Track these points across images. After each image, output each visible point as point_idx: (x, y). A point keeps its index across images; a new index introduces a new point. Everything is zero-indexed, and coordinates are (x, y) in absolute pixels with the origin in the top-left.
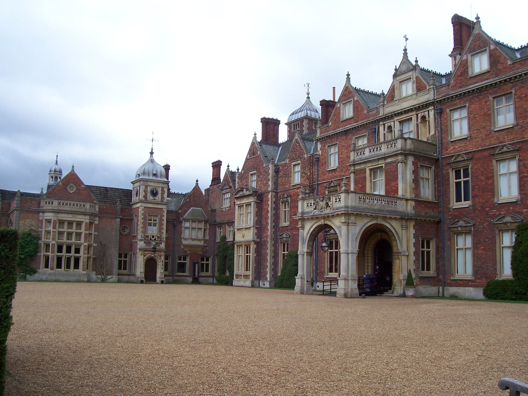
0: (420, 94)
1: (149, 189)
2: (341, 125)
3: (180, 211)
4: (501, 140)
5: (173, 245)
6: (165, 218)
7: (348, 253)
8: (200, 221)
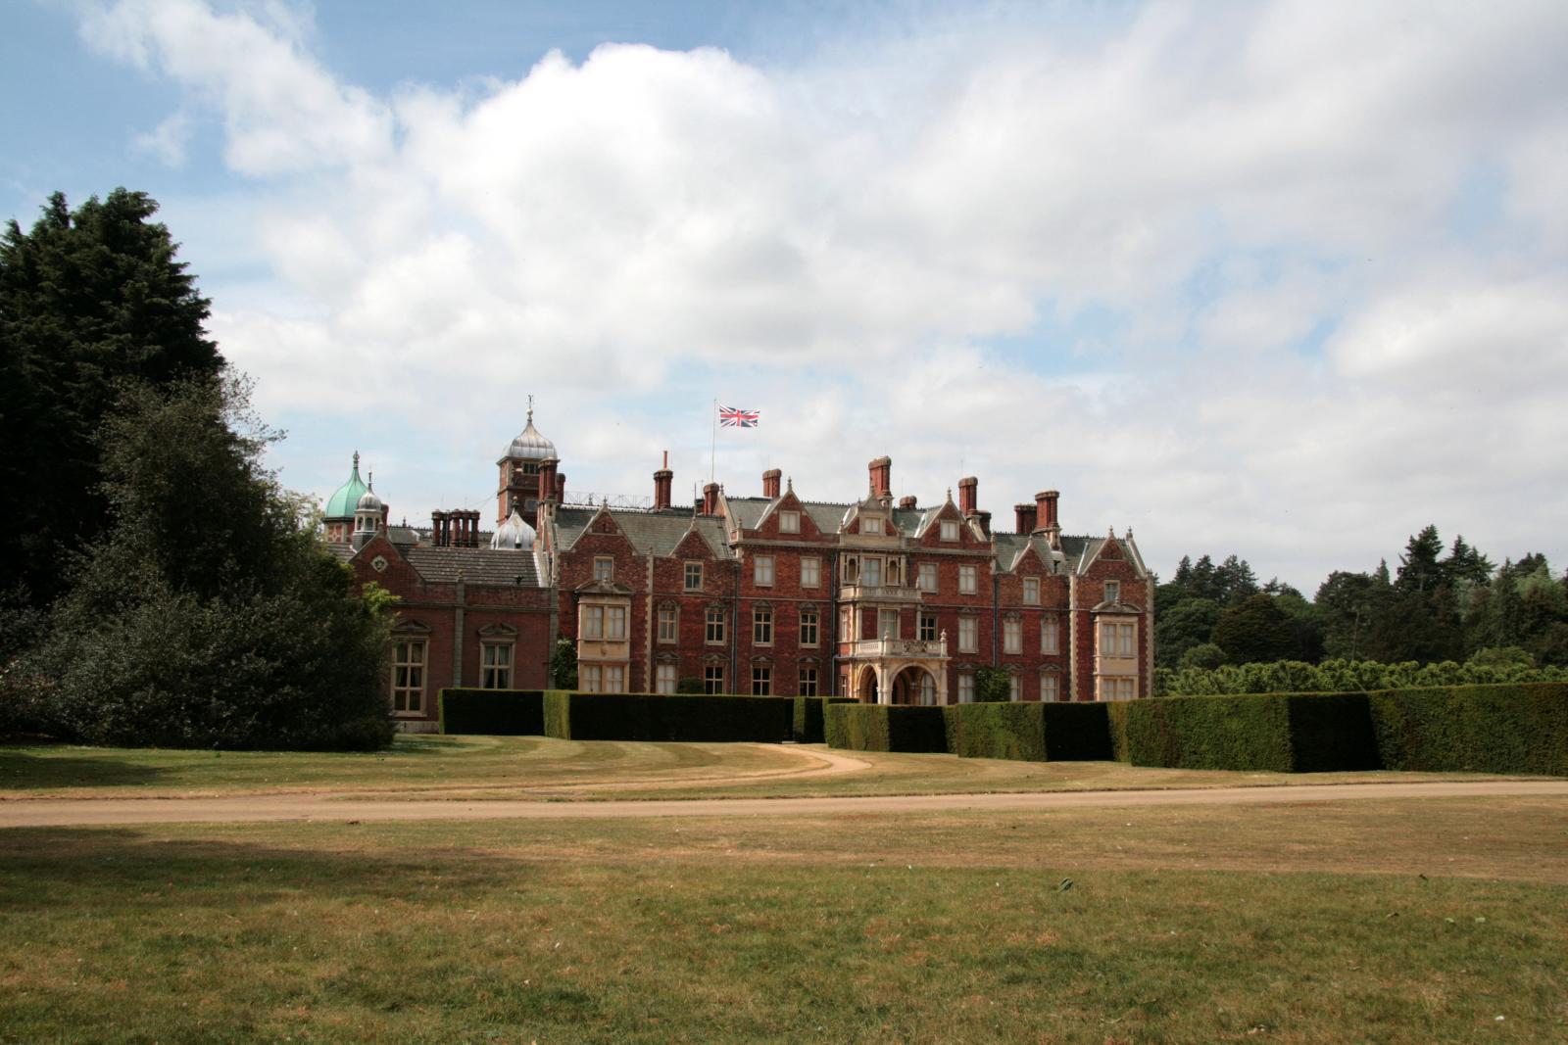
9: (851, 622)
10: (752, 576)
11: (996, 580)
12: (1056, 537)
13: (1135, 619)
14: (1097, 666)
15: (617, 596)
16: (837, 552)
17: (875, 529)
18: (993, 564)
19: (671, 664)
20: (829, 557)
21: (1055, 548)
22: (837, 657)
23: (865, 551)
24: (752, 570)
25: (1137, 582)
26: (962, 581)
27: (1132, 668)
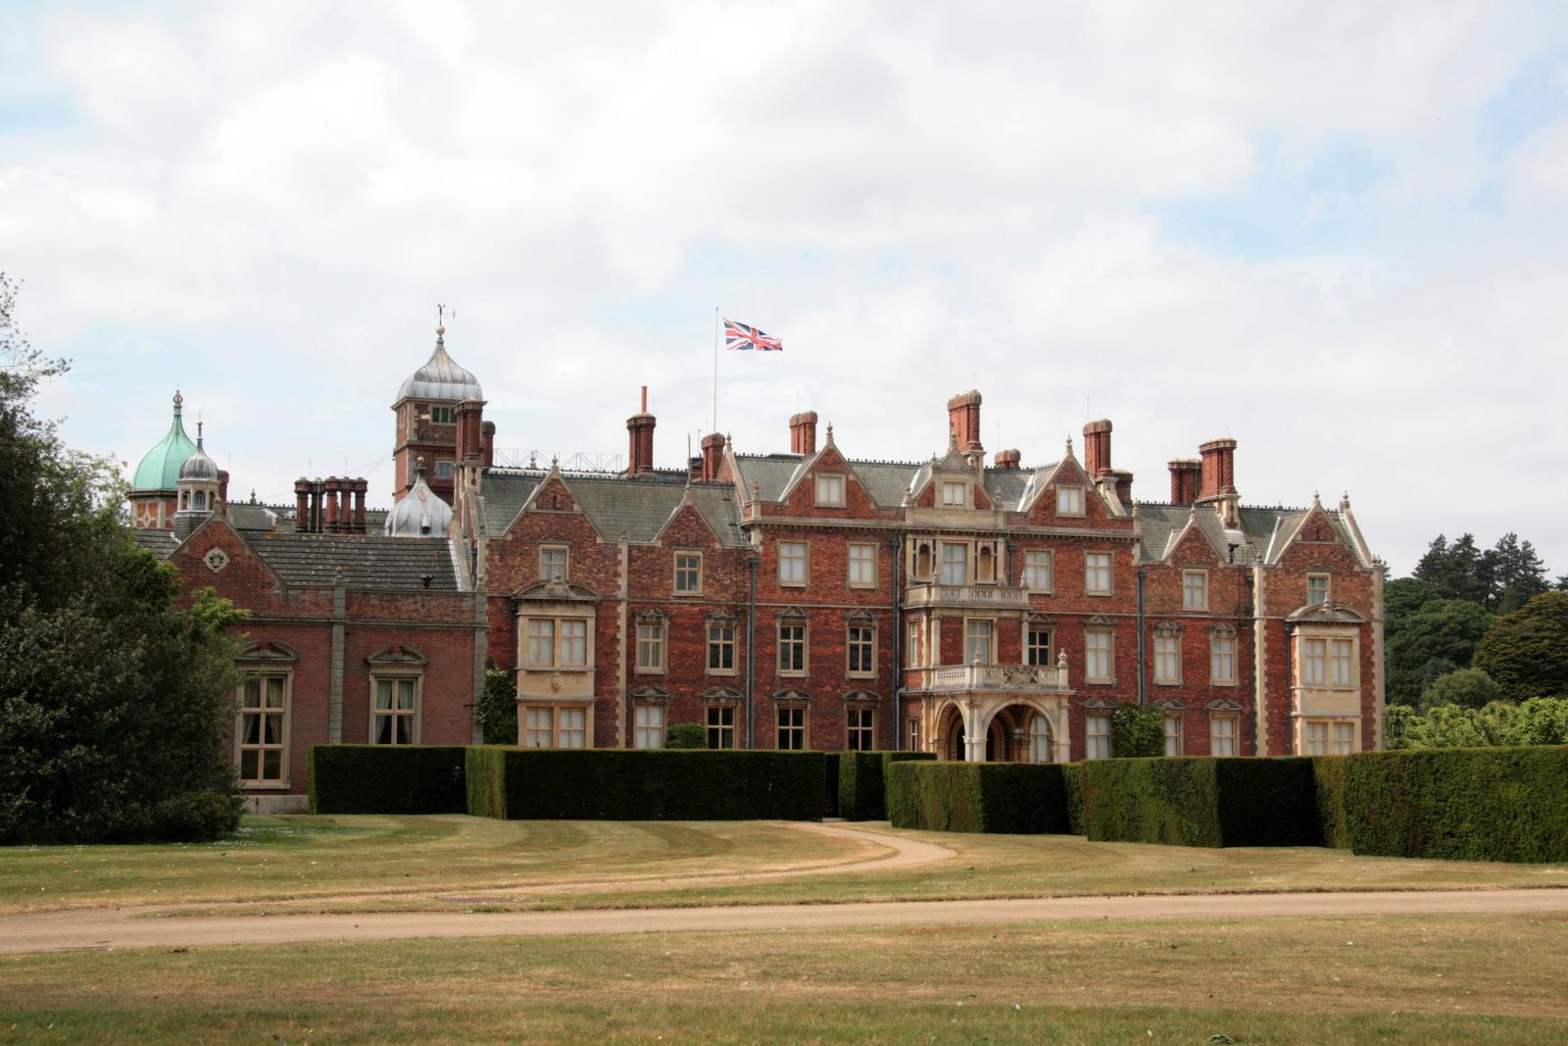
2: (815, 512)
4: (1095, 607)
9: (924, 638)
10: (775, 571)
11: (1140, 575)
12: (1231, 508)
13: (1354, 632)
14: (1297, 702)
15: (574, 603)
16: (902, 533)
17: (959, 499)
18: (1136, 551)
19: (655, 704)
20: (890, 541)
21: (1231, 525)
22: (902, 690)
23: (943, 533)
24: (776, 562)
25: (1358, 574)
26: (1090, 575)
27: (1352, 706)
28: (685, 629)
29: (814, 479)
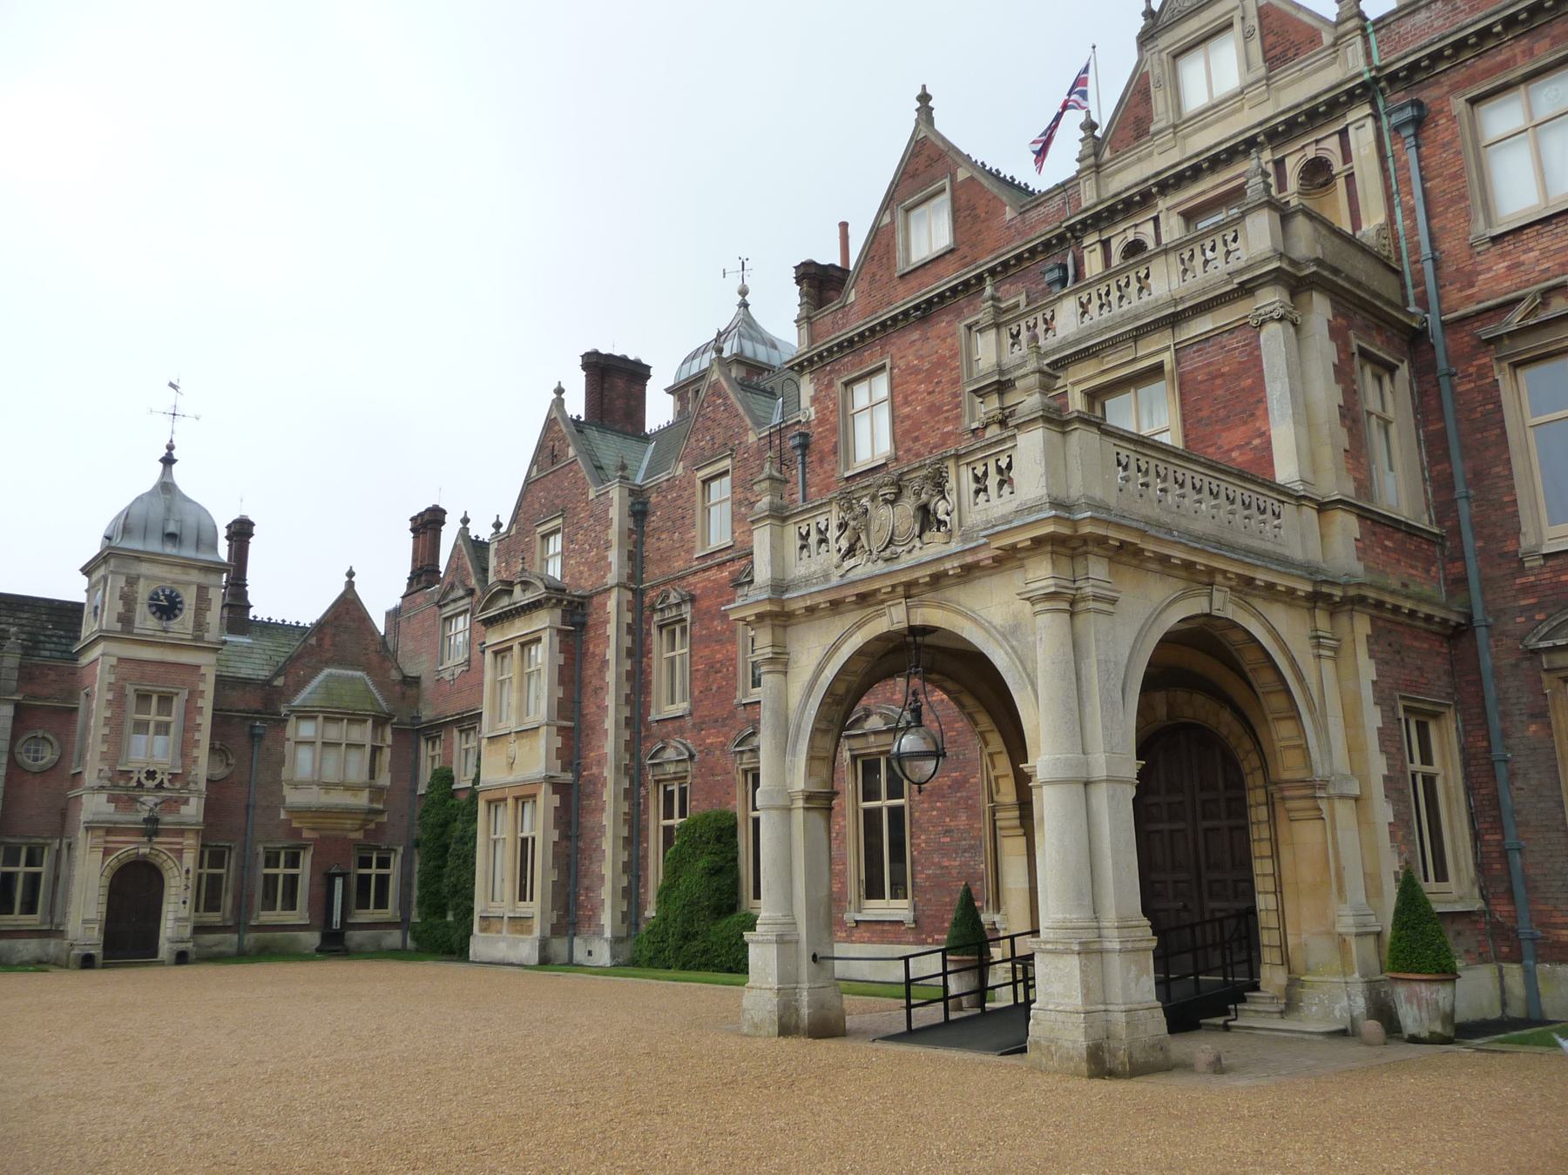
0: (1284, 76)
1: (143, 591)
3: (279, 682)
5: (247, 807)
6: (207, 703)
7: (1087, 784)
8: (355, 719)
28: (712, 619)
29: (893, 222)
